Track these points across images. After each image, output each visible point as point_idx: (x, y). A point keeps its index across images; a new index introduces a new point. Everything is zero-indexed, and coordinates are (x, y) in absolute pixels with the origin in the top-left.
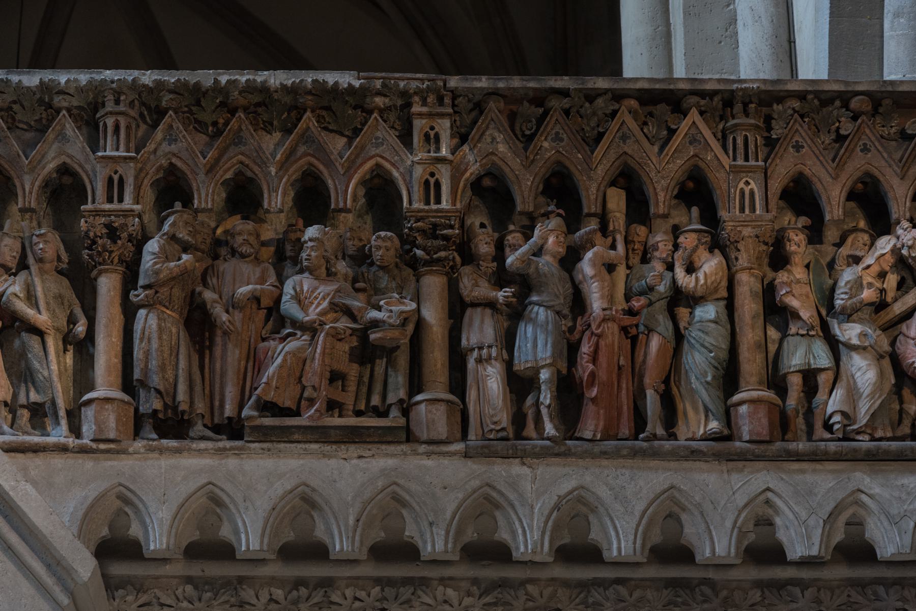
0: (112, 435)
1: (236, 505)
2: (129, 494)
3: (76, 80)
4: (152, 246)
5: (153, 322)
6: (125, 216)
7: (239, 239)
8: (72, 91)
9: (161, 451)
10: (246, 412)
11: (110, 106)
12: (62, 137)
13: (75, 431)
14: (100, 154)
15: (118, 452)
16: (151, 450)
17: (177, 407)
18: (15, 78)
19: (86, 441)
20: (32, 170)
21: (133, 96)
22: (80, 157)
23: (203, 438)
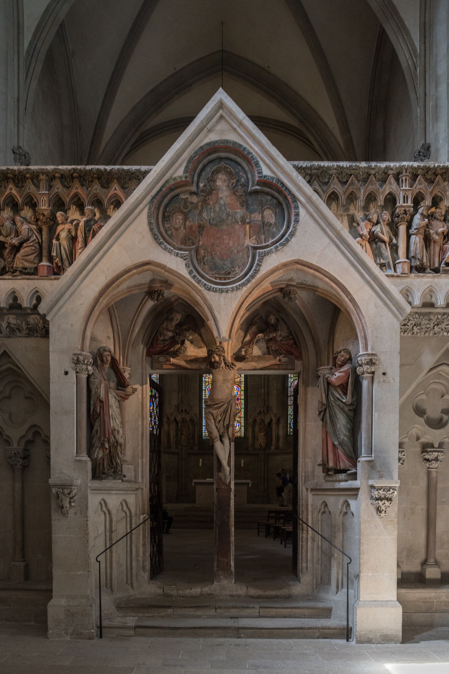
0: (406, 272)
1: (437, 291)
2: (409, 289)
3: (396, 165)
4: (417, 217)
5: (418, 239)
6: (409, 208)
7: (437, 215)
8: (394, 169)
9: (418, 276)
10: (442, 265)
11: (404, 173)
12: (390, 183)
13: (395, 271)
14: (402, 188)
15: (407, 277)
16: (416, 276)
17: (423, 264)
18: (379, 165)
19: (399, 274)
20: (382, 193)
21: (411, 170)
22: (395, 189)
23: (429, 273)
